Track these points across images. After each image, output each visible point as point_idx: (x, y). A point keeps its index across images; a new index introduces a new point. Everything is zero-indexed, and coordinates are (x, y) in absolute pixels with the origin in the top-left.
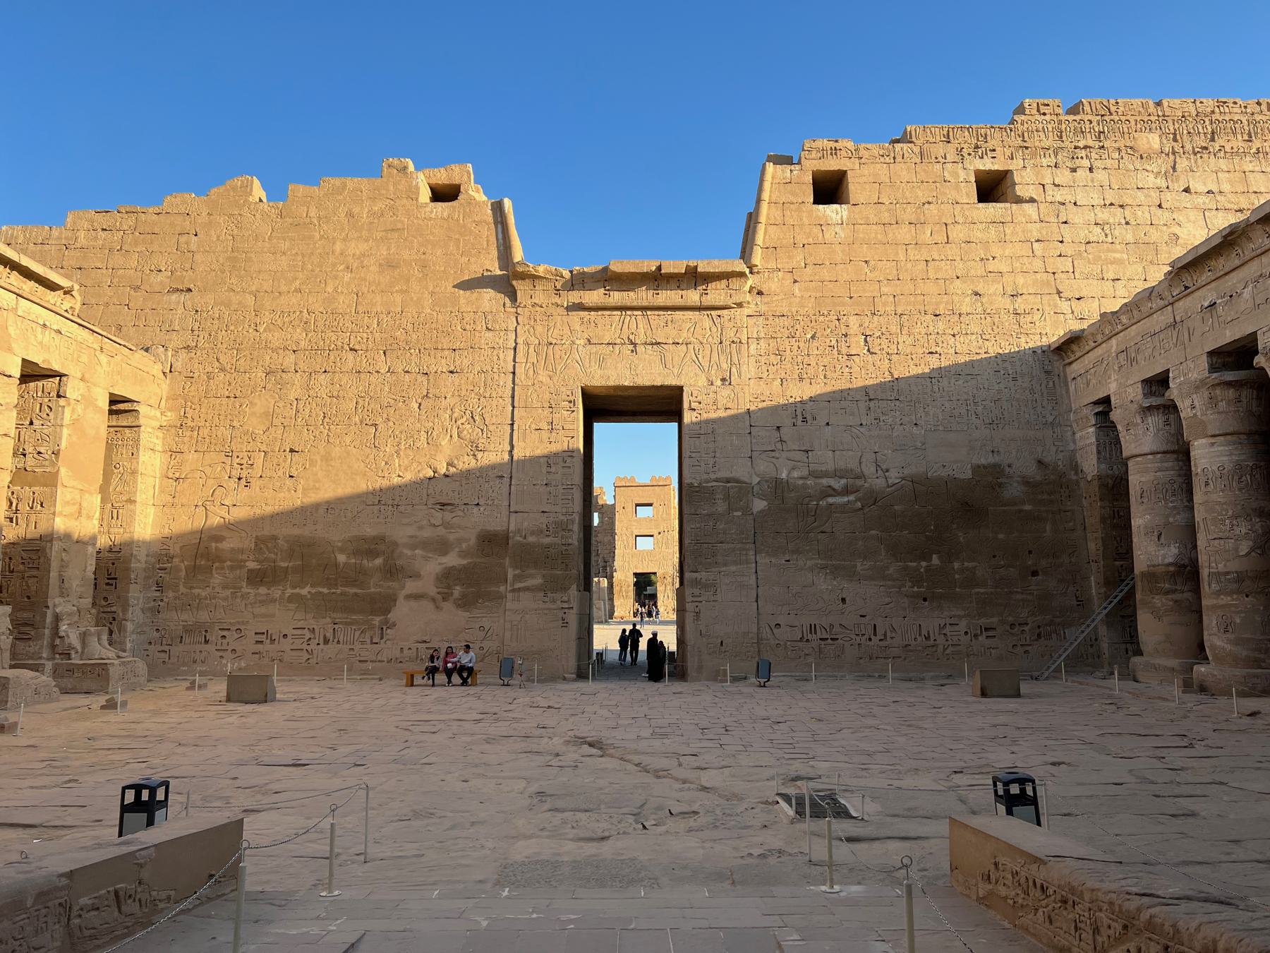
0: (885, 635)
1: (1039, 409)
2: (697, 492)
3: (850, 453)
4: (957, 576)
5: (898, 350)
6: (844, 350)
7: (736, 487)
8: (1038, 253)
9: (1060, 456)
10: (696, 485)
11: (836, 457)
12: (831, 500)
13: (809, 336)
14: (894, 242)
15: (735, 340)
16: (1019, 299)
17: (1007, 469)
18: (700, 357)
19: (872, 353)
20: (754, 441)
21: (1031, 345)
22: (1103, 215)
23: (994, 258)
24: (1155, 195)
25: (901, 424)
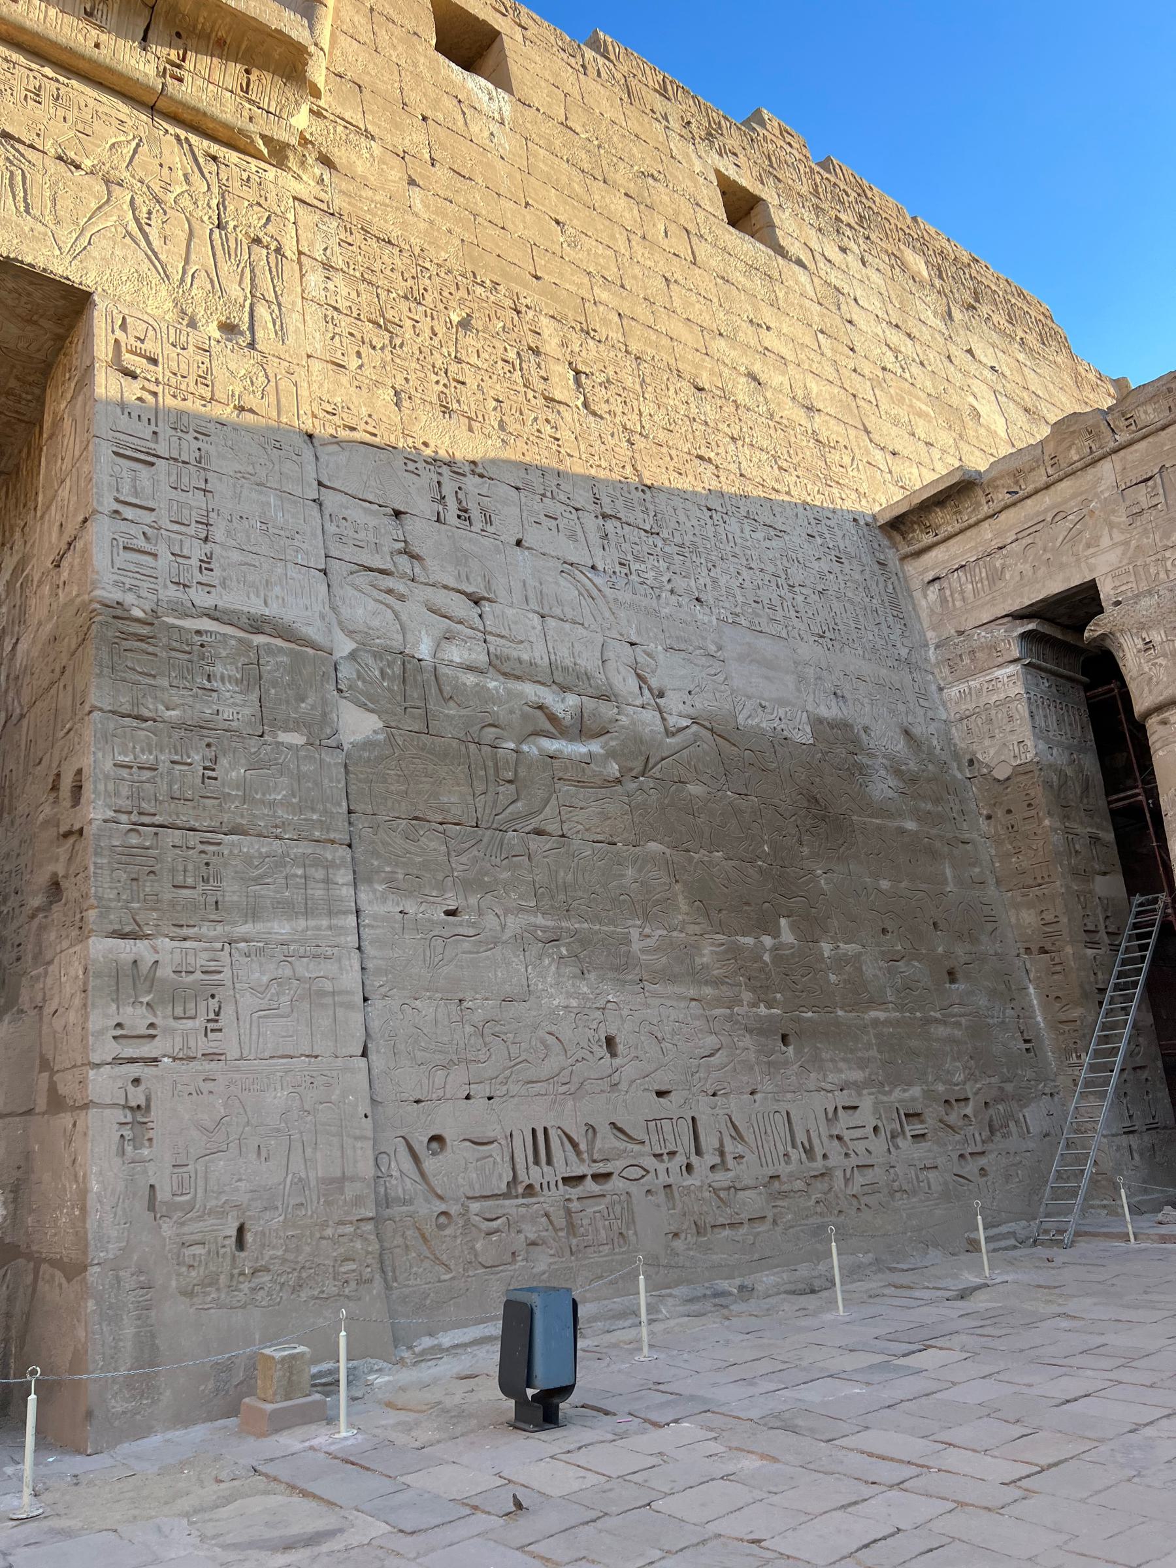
1: (886, 631)
2: (141, 639)
3: (580, 630)
4: (833, 978)
5: (643, 427)
7: (280, 649)
8: (829, 353)
10: (137, 613)
11: (550, 633)
13: (455, 319)
17: (864, 736)
18: (153, 233)
19: (594, 414)
20: (331, 529)
21: (847, 505)
22: (894, 337)
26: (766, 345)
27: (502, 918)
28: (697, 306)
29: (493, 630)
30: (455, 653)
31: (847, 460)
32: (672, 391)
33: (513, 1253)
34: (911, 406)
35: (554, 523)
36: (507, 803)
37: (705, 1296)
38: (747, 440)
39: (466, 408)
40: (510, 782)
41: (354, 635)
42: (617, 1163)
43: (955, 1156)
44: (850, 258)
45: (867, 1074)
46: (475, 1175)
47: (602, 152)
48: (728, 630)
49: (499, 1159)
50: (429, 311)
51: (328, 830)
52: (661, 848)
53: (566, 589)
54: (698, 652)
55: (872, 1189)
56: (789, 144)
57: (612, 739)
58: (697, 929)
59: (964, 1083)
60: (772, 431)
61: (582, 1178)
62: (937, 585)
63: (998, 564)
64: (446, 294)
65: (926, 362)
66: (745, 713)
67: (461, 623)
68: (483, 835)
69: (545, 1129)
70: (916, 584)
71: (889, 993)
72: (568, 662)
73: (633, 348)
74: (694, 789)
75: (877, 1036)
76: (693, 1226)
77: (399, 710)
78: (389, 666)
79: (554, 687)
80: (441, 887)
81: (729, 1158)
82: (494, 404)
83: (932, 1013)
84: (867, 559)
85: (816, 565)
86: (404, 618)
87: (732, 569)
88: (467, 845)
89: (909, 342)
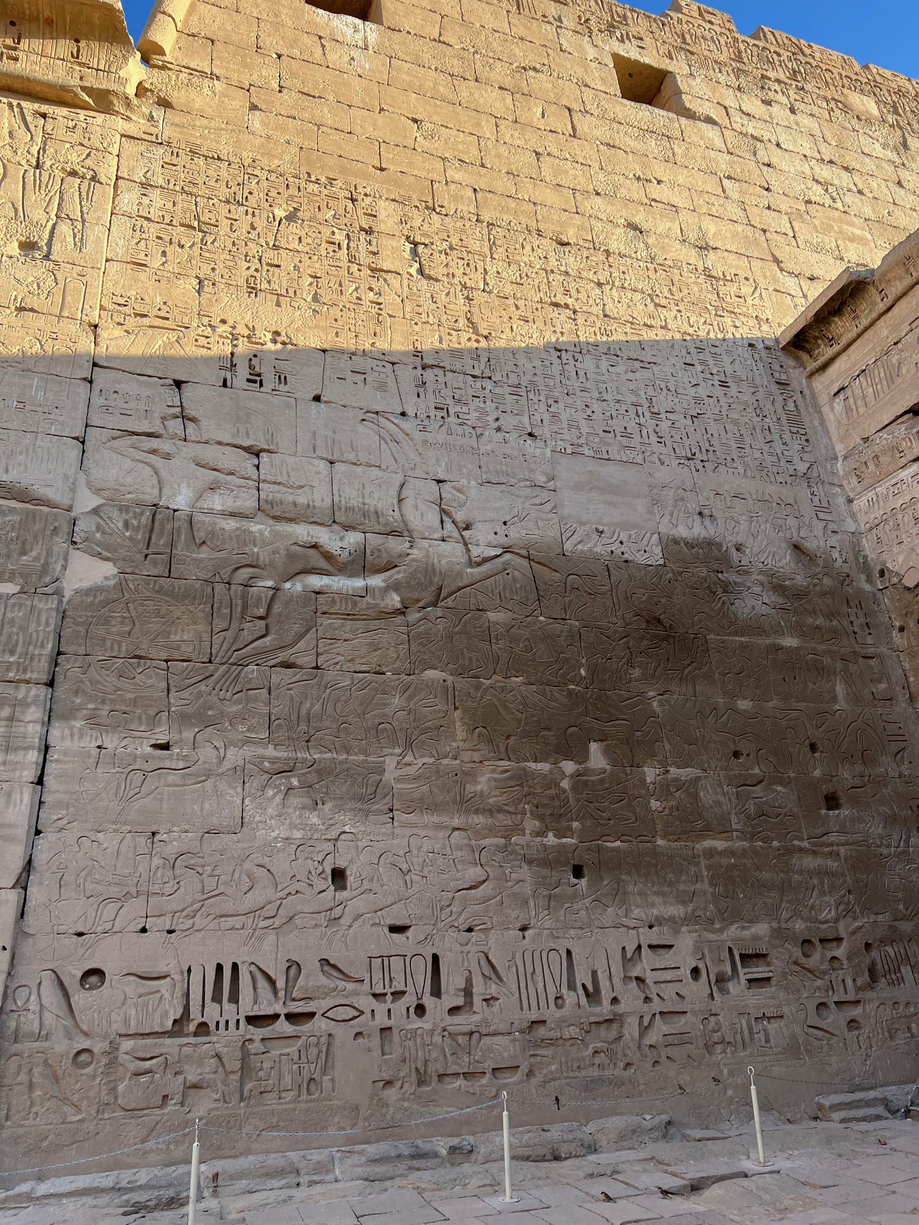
0: (468, 992)
1: (778, 447)
4: (655, 804)
5: (487, 284)
6: (364, 257)
7: (12, 510)
8: (735, 196)
9: (834, 540)
12: (316, 581)
13: (280, 213)
14: (472, 106)
15: (81, 171)
16: (712, 255)
19: (429, 278)
20: (97, 401)
22: (824, 173)
23: (659, 182)
24: (890, 169)
25: (498, 429)
26: (653, 197)
27: (222, 751)
28: (571, 172)
29: (269, 478)
30: (217, 502)
31: (746, 290)
32: (528, 248)
33: (165, 1097)
34: (841, 232)
35: (362, 377)
36: (251, 638)
37: (399, 1156)
38: (616, 284)
39: (276, 287)
40: (261, 618)
41: (101, 493)
42: (323, 1002)
43: (812, 1007)
44: (775, 109)
45: (689, 909)
46: (133, 1011)
47: (477, 56)
48: (564, 461)
49: (167, 995)
50: (250, 211)
51: (25, 671)
52: (443, 675)
53: (366, 435)
54: (522, 484)
55: (681, 1039)
56: (710, 22)
57: (399, 572)
58: (477, 756)
59: (837, 921)
60: (651, 273)
61: (276, 1017)
62: (842, 396)
63: (895, 360)
64: (273, 193)
65: (866, 191)
66: (574, 539)
67: (233, 474)
68: (216, 670)
69: (235, 966)
70: (823, 399)
71: (734, 819)
72: (353, 503)
73: (486, 217)
74: (492, 616)
75: (709, 868)
76: (414, 1074)
77: (140, 557)
78: (135, 518)
79: (335, 527)
80: (153, 722)
81: (477, 1001)
82: (310, 280)
83: (796, 842)
84: (763, 380)
85: (692, 392)
86: (164, 474)
87: (579, 403)
88: (193, 681)
89: (845, 175)
